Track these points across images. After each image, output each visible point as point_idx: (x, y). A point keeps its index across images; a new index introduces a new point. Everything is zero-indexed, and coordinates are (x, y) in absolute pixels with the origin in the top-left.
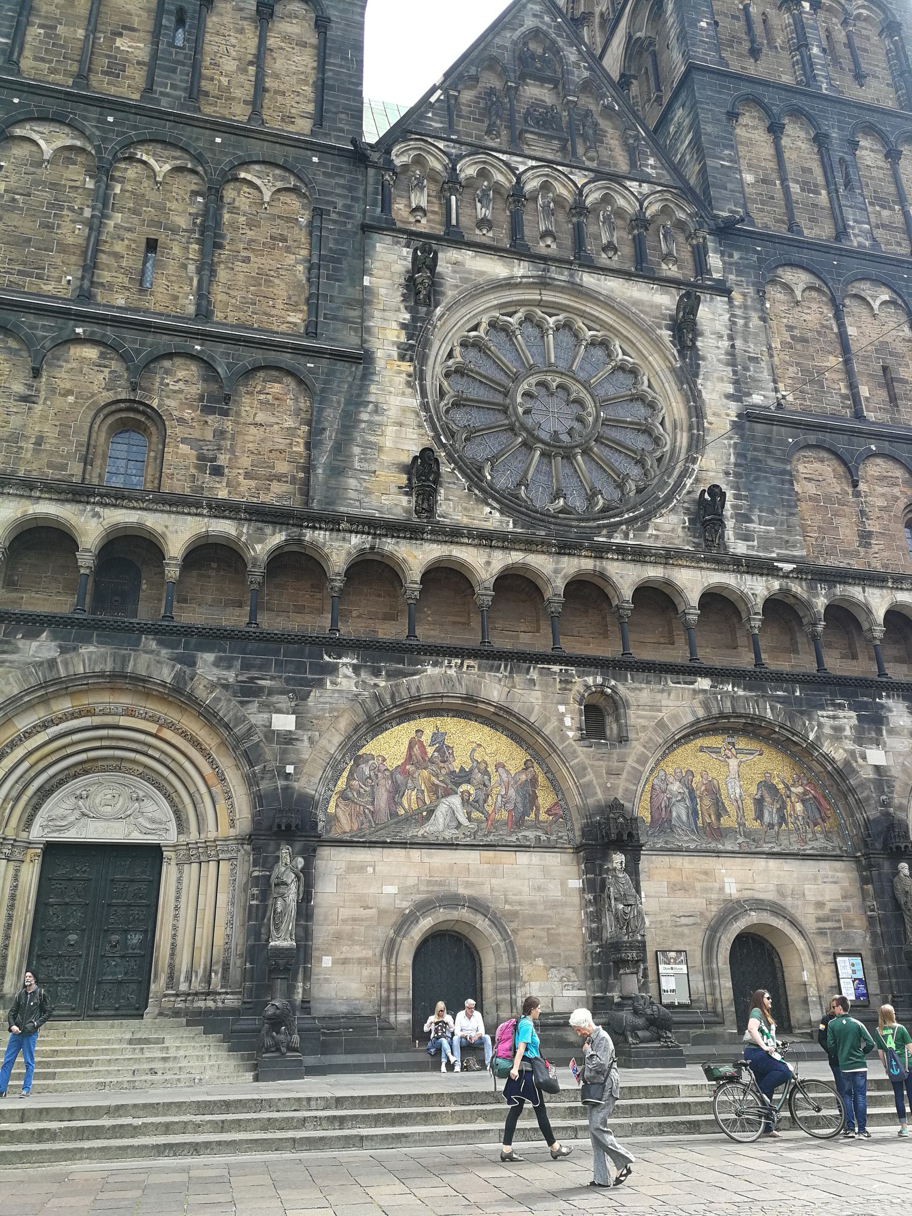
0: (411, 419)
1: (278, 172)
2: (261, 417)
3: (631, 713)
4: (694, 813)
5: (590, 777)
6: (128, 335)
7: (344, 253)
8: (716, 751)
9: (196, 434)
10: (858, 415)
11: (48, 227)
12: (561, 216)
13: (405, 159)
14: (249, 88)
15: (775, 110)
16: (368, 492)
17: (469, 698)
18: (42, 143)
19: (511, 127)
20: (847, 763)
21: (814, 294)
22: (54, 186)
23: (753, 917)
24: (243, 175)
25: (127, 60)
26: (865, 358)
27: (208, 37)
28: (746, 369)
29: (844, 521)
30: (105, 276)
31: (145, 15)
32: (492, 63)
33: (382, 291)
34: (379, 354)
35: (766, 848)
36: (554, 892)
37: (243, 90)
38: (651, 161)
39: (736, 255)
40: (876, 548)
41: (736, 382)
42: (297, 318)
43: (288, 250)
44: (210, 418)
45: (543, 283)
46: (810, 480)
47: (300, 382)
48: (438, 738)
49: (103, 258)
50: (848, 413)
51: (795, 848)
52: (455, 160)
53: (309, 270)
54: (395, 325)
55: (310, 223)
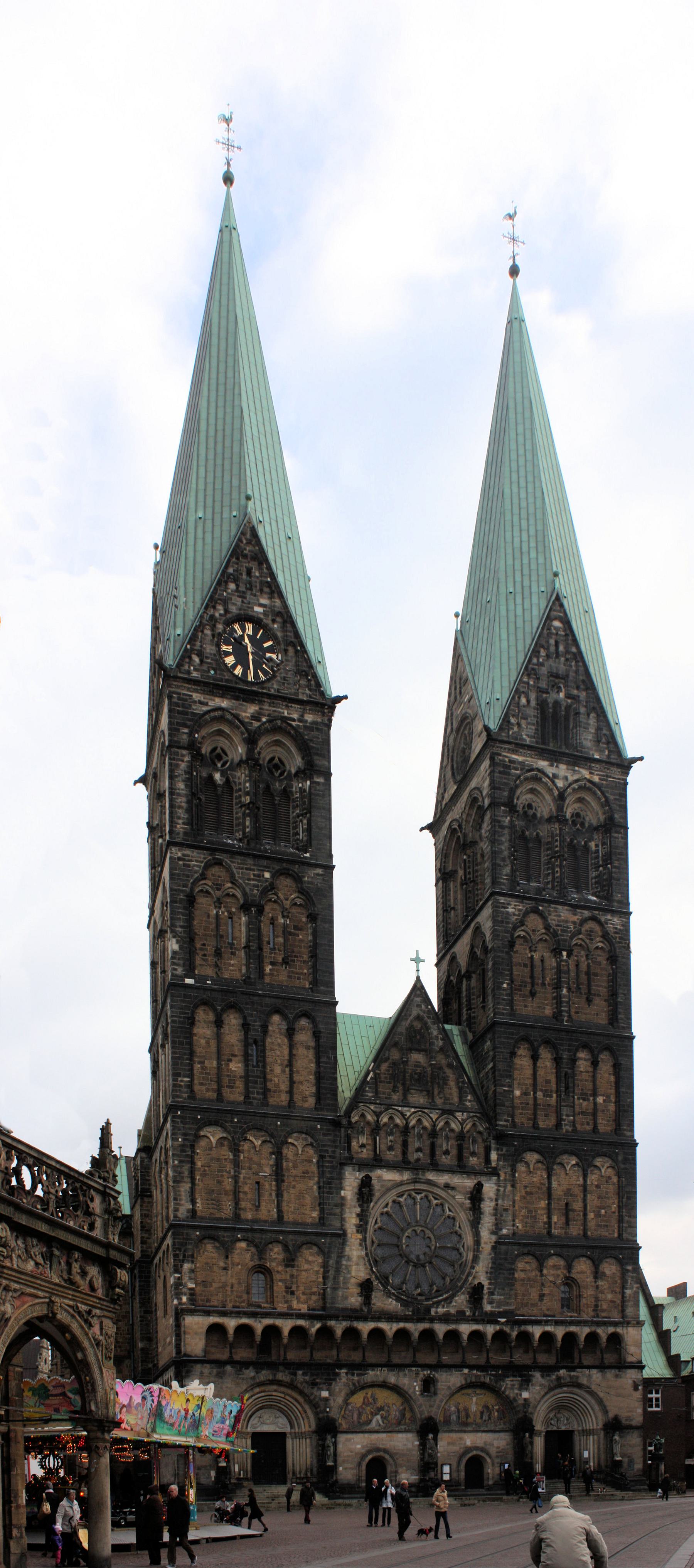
0: (362, 1262)
1: (304, 1136)
2: (306, 1266)
3: (439, 1384)
4: (458, 1417)
5: (424, 1407)
6: (258, 1235)
7: (332, 1178)
8: (469, 1395)
9: (284, 1277)
10: (549, 1233)
11: (219, 1182)
12: (425, 1137)
13: (356, 1118)
14: (288, 1083)
15: (536, 1044)
16: (346, 1298)
17: (384, 1382)
18: (211, 1138)
19: (404, 1084)
20: (514, 1398)
21: (540, 1165)
22: (218, 1160)
23: (475, 1453)
24: (290, 1140)
25: (235, 1076)
26: (559, 1199)
27: (268, 1053)
28: (502, 1216)
29: (534, 1290)
30: (243, 1204)
31: (239, 1044)
32: (396, 1045)
33: (349, 1198)
34: (349, 1231)
35: (482, 1429)
36: (410, 1446)
37: (284, 1087)
38: (469, 1097)
39: (504, 1149)
40: (545, 1301)
41: (496, 1225)
42: (315, 1214)
43: (310, 1178)
44: (288, 1269)
45: (415, 1181)
46: (522, 1271)
47: (319, 1248)
48: (373, 1396)
49: (241, 1195)
50: (545, 1232)
51: (493, 1428)
52: (378, 1115)
53: (319, 1188)
54: (354, 1215)
55: (318, 1162)
